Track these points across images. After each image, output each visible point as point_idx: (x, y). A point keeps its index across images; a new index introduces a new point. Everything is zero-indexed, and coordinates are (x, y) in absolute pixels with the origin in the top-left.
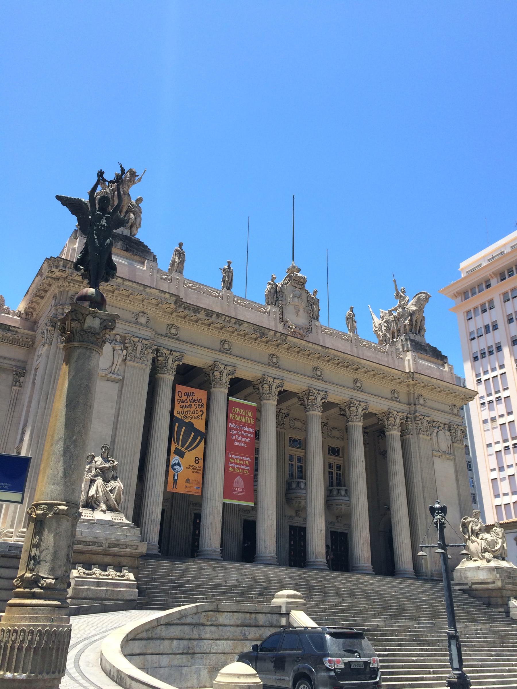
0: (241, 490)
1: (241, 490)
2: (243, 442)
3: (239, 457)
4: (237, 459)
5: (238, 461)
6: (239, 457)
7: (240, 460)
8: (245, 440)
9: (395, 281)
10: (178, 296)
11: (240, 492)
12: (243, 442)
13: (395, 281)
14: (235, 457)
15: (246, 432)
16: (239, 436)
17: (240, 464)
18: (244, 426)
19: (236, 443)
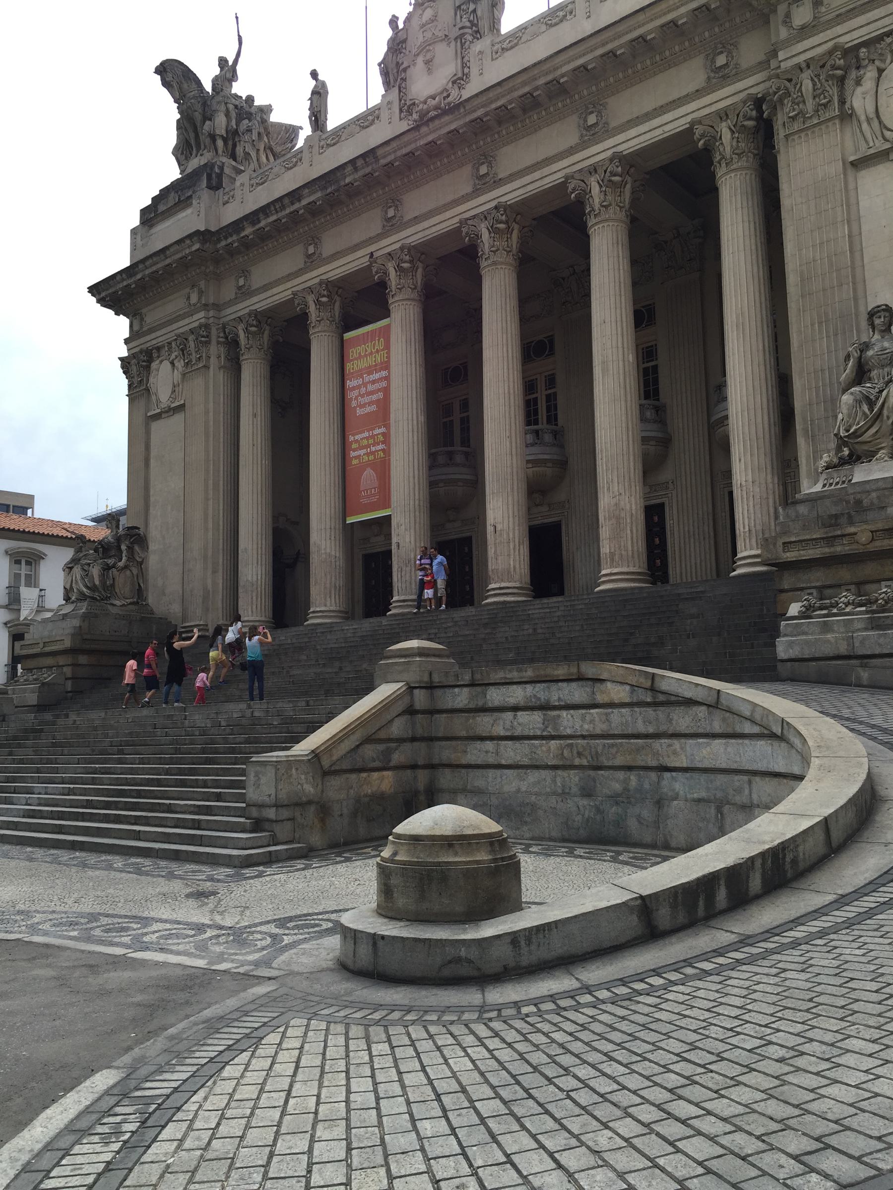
0: (373, 491)
1: (373, 491)
2: (370, 404)
3: (366, 434)
4: (362, 439)
5: (365, 442)
6: (366, 434)
7: (367, 438)
8: (374, 397)
10: (198, 233)
11: (374, 495)
12: (370, 404)
14: (357, 437)
15: (373, 382)
16: (362, 396)
17: (368, 446)
18: (370, 373)
19: (359, 412)
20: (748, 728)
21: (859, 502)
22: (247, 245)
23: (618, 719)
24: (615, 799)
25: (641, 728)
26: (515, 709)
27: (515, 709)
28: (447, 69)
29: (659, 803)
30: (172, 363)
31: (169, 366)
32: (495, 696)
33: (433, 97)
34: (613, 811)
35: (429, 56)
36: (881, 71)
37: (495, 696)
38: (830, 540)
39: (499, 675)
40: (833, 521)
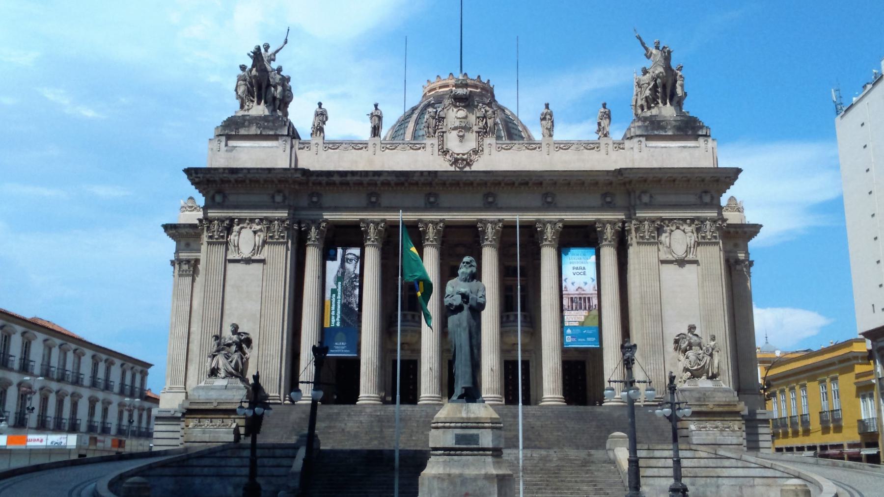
9: (639, 38)
13: (639, 38)
20: (753, 465)
21: (705, 394)
22: (328, 184)
23: (703, 462)
24: (703, 486)
25: (711, 465)
26: (665, 458)
27: (665, 458)
28: (471, 142)
29: (718, 487)
30: (255, 232)
31: (252, 234)
32: (657, 454)
33: (463, 154)
34: (701, 489)
35: (461, 134)
36: (672, 231)
37: (657, 454)
38: (700, 405)
39: (660, 447)
40: (699, 399)
